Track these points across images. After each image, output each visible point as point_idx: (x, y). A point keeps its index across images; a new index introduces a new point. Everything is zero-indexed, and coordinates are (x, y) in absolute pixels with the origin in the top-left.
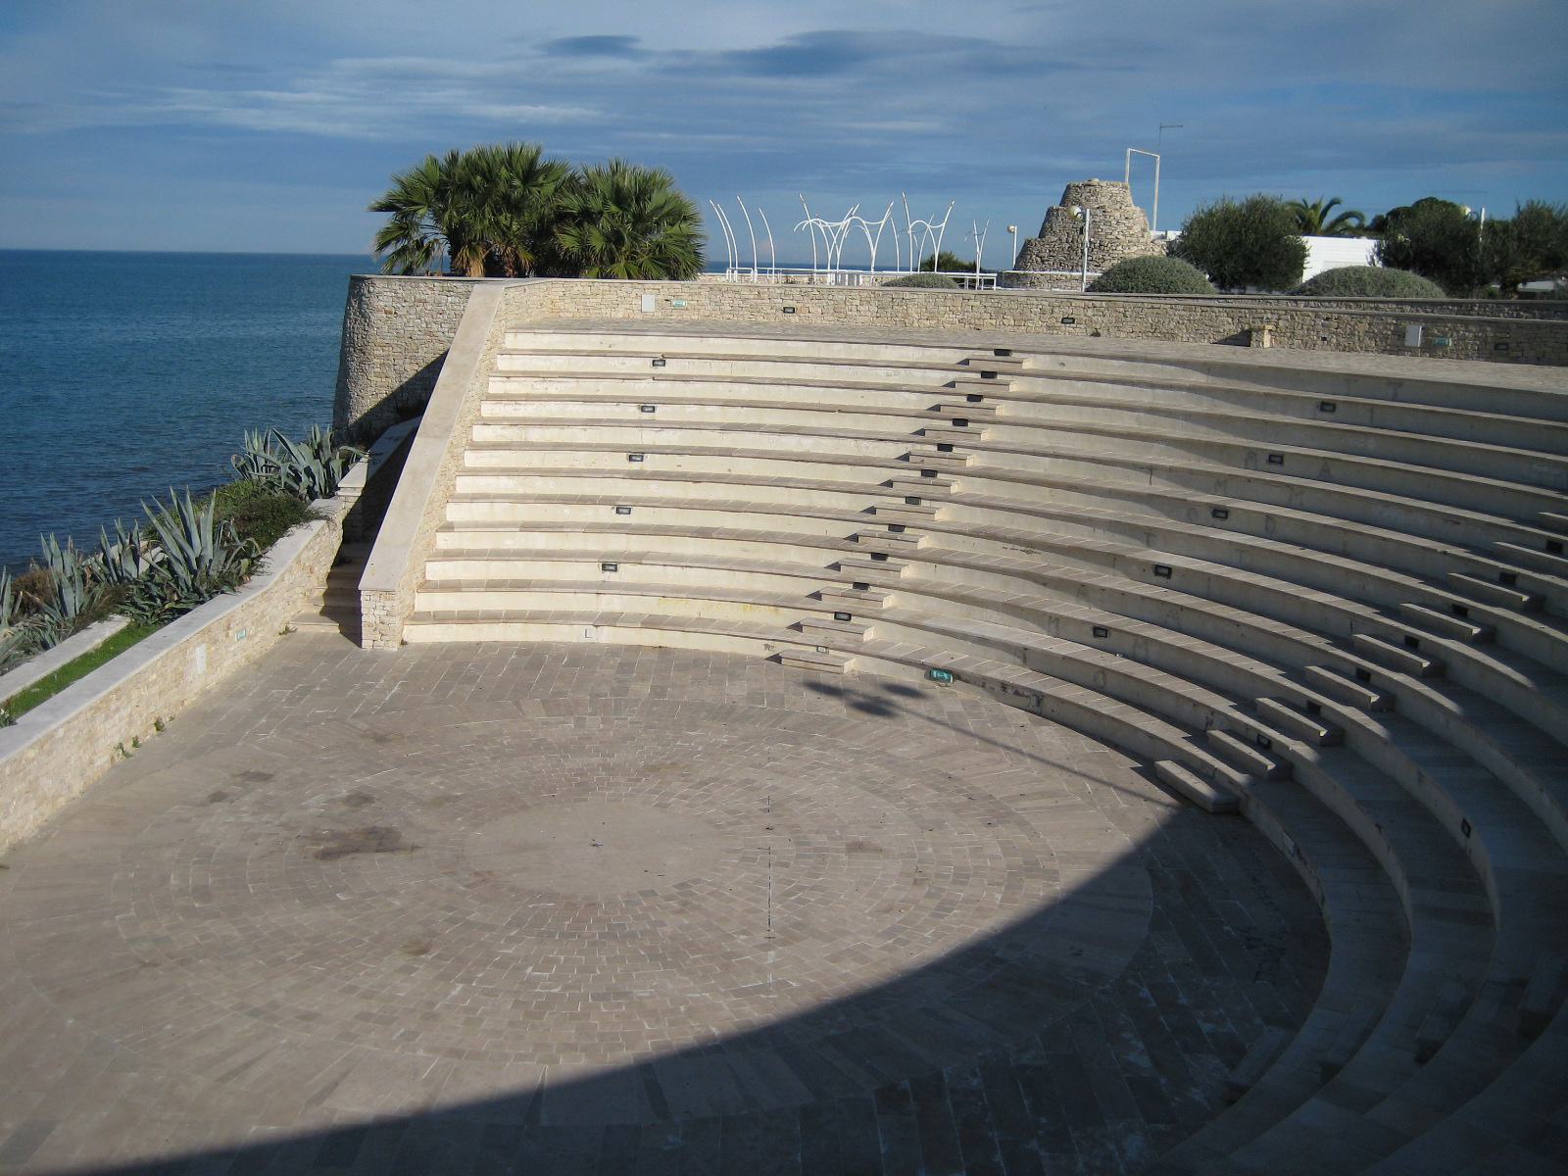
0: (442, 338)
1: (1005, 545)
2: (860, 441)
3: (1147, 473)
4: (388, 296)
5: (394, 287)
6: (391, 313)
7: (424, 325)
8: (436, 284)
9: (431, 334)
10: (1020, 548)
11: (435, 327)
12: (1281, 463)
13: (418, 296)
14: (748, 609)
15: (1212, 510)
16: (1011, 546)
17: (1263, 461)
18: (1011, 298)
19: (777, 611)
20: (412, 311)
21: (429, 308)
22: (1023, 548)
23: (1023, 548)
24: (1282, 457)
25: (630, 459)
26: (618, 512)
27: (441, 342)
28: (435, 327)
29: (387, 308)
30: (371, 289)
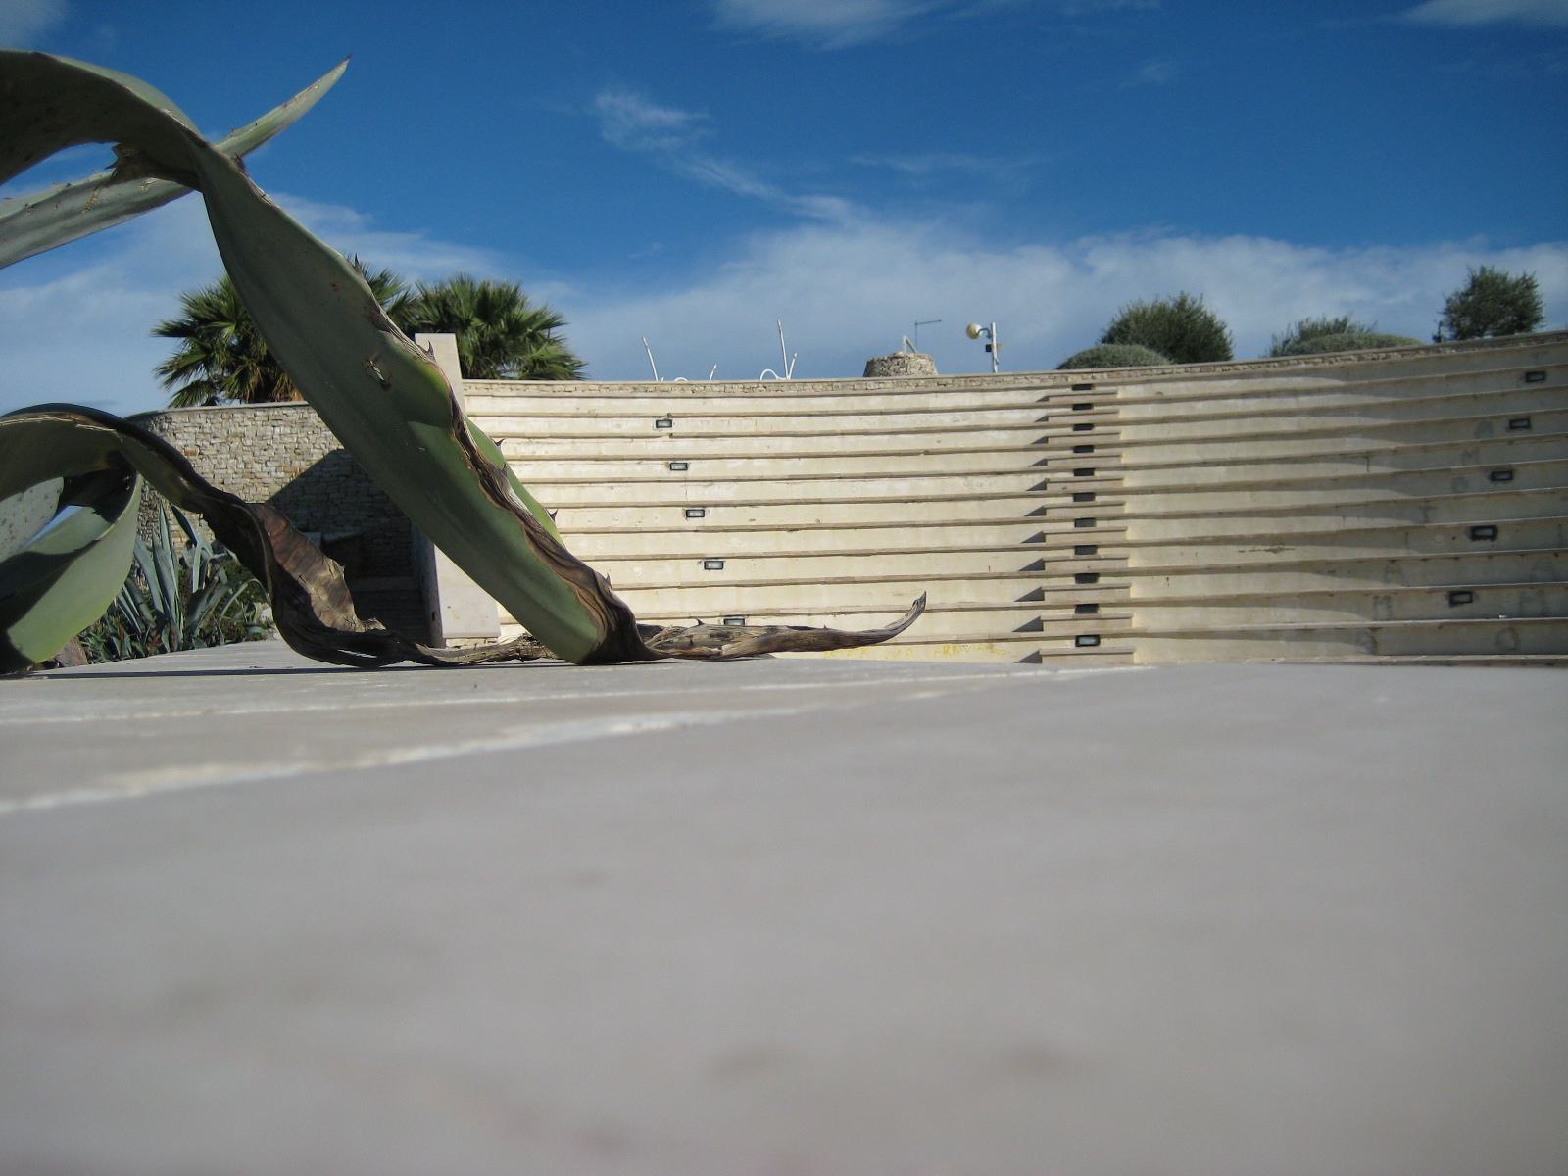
0: (269, 481)
1: (1241, 548)
2: (970, 478)
3: (1363, 463)
4: (189, 433)
5: (198, 421)
6: (194, 454)
7: (242, 466)
8: (258, 413)
9: (252, 476)
10: (1263, 548)
11: (257, 467)
12: (1528, 427)
13: (233, 430)
14: (951, 651)
15: (1489, 474)
16: (1250, 547)
17: (1500, 432)
18: (996, 379)
19: (991, 647)
20: (225, 449)
21: (249, 442)
22: (1268, 547)
23: (1268, 547)
24: (1528, 420)
25: (687, 515)
26: (706, 568)
27: (265, 485)
28: (257, 467)
29: (188, 449)
30: (165, 426)
